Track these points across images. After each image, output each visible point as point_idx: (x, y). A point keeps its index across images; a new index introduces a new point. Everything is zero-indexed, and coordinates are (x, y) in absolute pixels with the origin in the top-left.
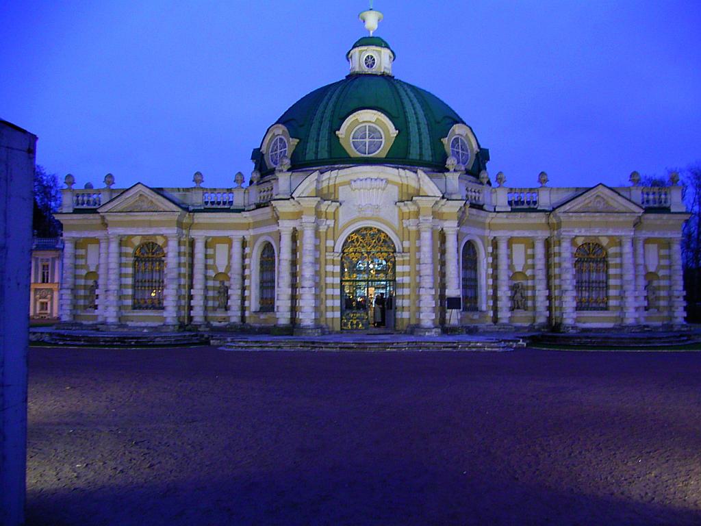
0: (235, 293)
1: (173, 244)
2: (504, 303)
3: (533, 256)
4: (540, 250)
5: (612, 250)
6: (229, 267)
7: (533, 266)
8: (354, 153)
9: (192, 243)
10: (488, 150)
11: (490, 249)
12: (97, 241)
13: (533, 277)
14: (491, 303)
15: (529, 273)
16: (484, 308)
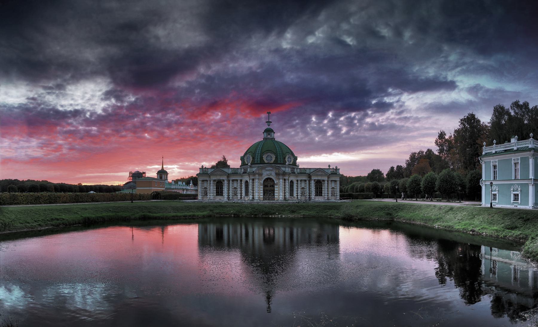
0: (239, 192)
1: (226, 182)
2: (299, 194)
3: (306, 184)
4: (307, 182)
5: (323, 183)
6: (237, 186)
7: (306, 186)
8: (266, 161)
9: (229, 181)
10: (297, 157)
11: (296, 182)
12: (207, 181)
13: (306, 188)
14: (296, 194)
15: (305, 188)
16: (295, 196)
